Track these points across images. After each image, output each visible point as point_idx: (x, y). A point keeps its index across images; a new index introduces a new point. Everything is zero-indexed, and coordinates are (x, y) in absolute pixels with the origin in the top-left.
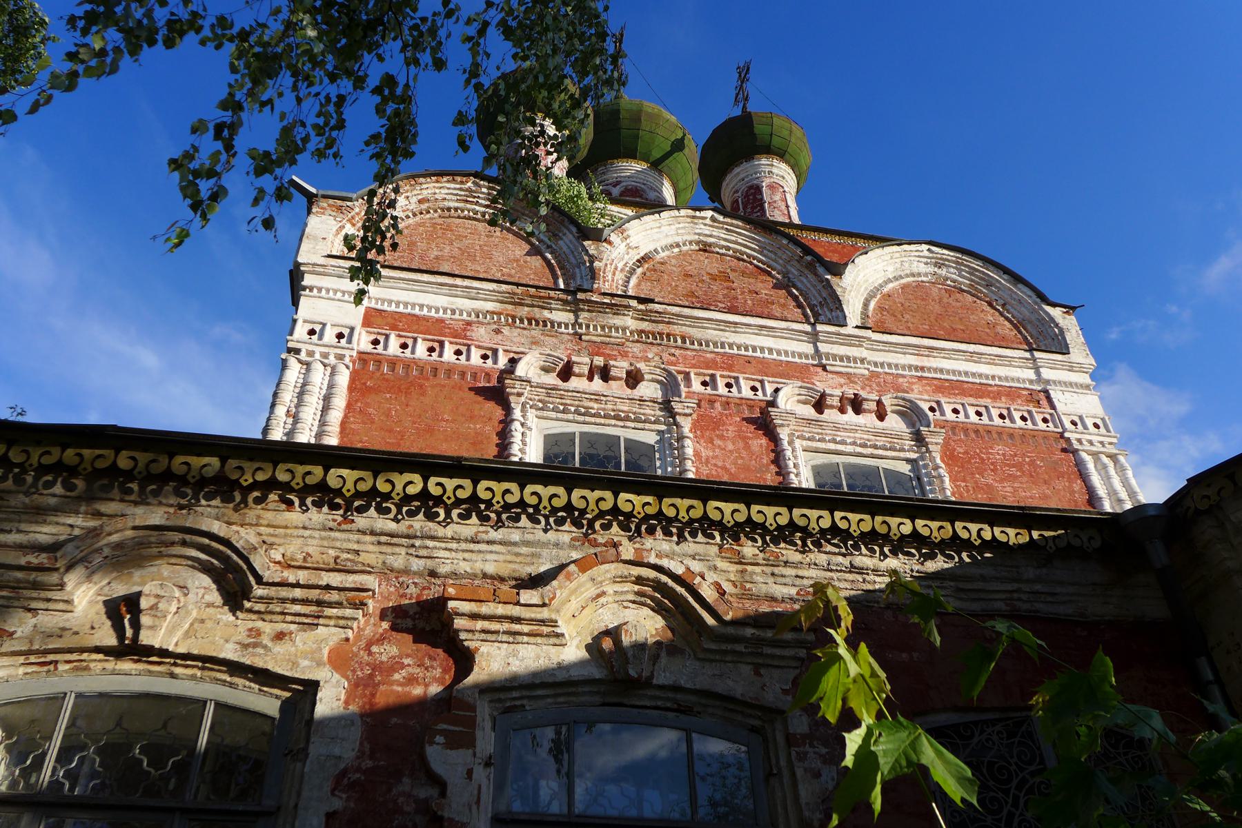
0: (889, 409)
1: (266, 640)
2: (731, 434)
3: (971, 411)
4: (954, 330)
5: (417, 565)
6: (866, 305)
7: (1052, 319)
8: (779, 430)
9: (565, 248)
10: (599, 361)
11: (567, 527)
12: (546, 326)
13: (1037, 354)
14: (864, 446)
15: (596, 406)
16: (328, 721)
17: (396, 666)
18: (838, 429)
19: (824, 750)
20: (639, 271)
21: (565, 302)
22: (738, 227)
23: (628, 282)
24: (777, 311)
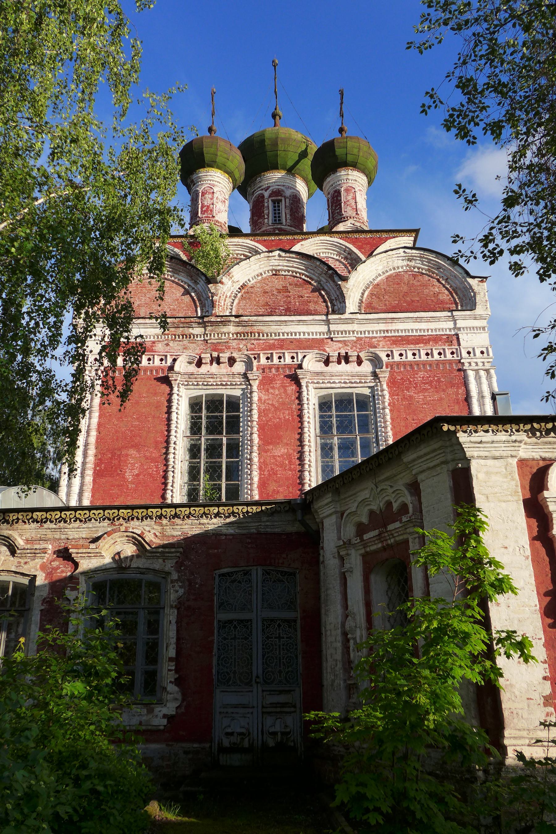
0: (363, 359)
1: (22, 565)
2: (278, 385)
3: (410, 354)
4: (413, 301)
5: (63, 537)
6: (363, 294)
7: (471, 287)
8: (301, 381)
9: (200, 289)
10: (215, 354)
11: (106, 521)
12: (190, 337)
13: (455, 313)
14: (345, 383)
15: (212, 380)
16: (38, 587)
17: (58, 568)
18: (333, 376)
20: (239, 295)
21: (199, 323)
22: (293, 258)
23: (233, 303)
24: (312, 307)
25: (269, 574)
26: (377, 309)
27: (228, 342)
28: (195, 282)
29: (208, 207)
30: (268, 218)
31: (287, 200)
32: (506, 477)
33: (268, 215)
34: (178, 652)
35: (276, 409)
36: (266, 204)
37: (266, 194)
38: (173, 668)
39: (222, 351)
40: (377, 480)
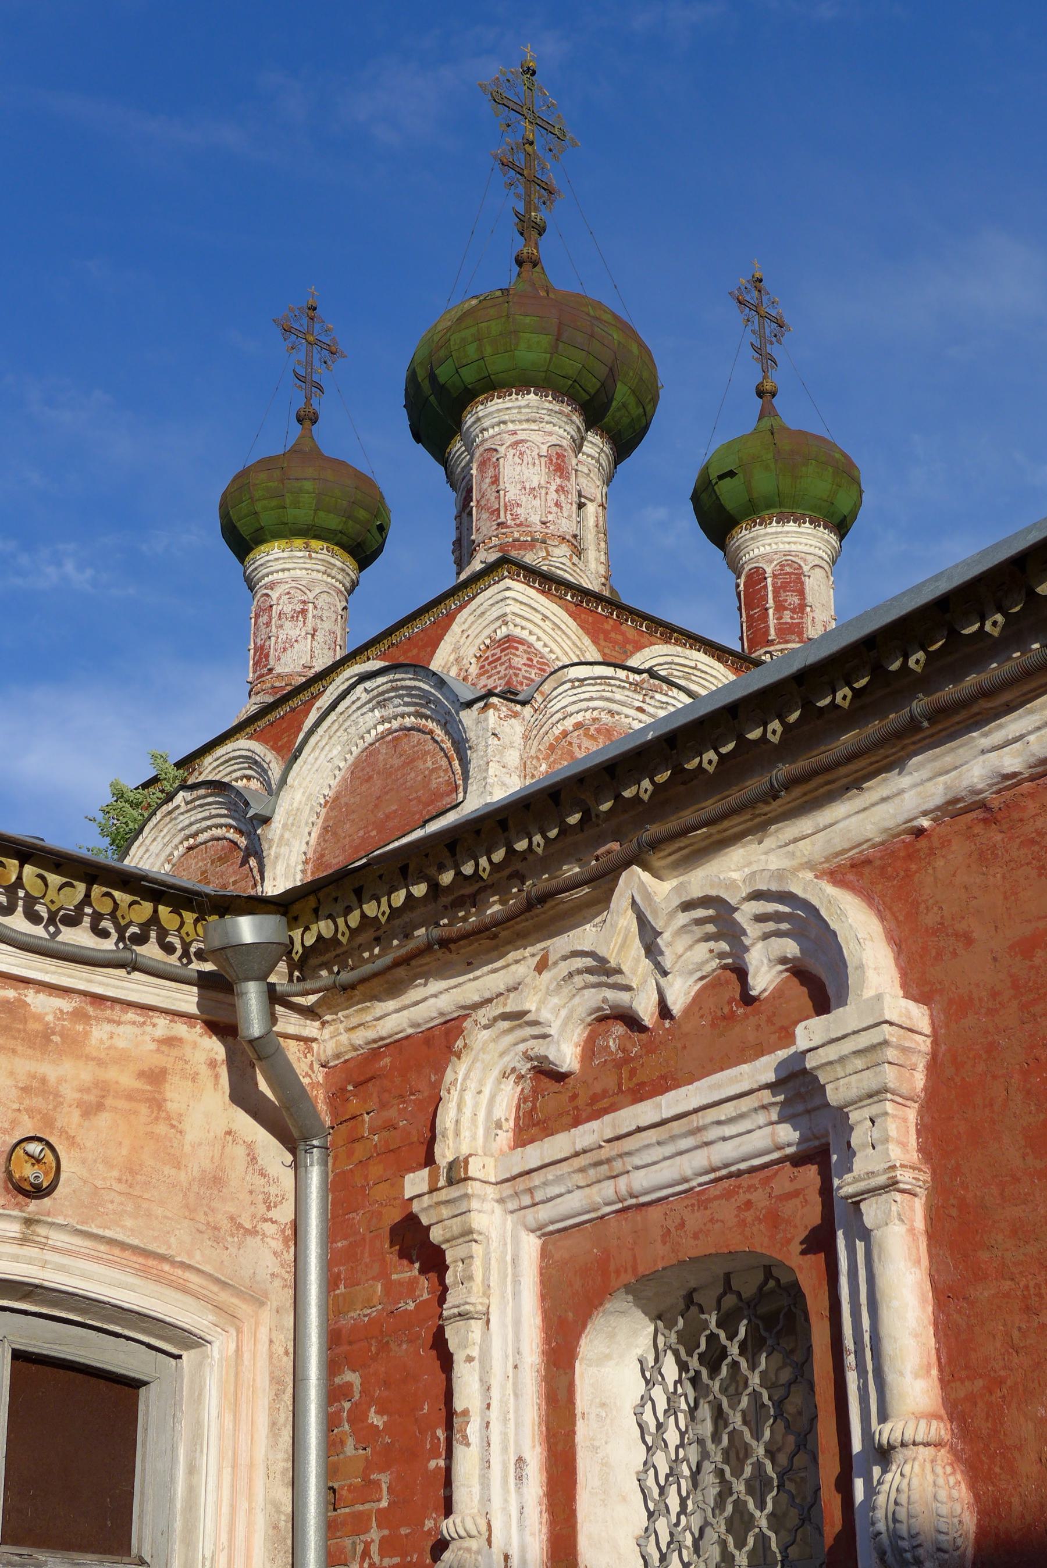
22: (205, 797)
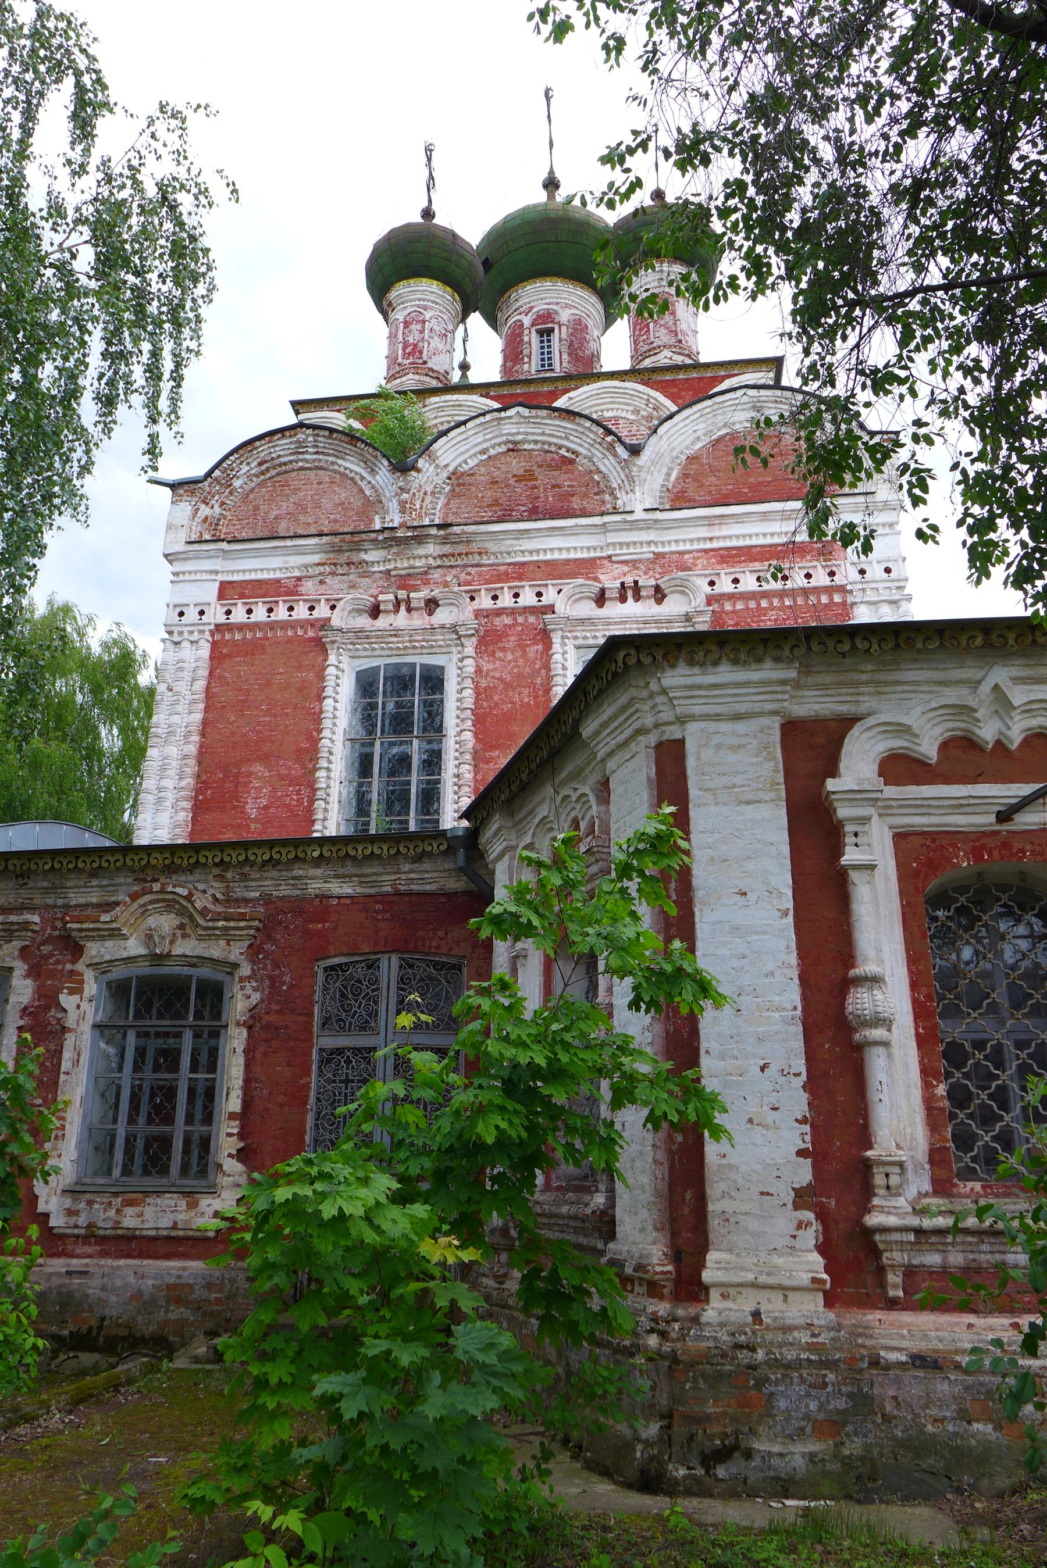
2: (511, 645)
5: (60, 902)
15: (395, 640)
17: (51, 955)
18: (610, 624)
19: (255, 984)
22: (543, 418)
25: (411, 966)
26: (695, 501)
27: (426, 573)
28: (373, 470)
29: (415, 345)
30: (529, 362)
31: (564, 329)
32: (757, 755)
33: (529, 357)
34: (246, 1104)
35: (508, 686)
36: (526, 339)
37: (527, 321)
38: (235, 1131)
39: (416, 589)
40: (557, 781)
